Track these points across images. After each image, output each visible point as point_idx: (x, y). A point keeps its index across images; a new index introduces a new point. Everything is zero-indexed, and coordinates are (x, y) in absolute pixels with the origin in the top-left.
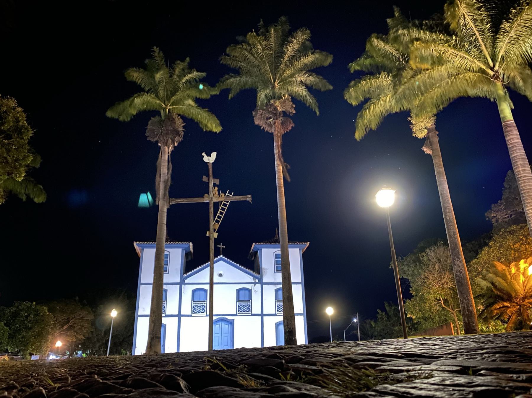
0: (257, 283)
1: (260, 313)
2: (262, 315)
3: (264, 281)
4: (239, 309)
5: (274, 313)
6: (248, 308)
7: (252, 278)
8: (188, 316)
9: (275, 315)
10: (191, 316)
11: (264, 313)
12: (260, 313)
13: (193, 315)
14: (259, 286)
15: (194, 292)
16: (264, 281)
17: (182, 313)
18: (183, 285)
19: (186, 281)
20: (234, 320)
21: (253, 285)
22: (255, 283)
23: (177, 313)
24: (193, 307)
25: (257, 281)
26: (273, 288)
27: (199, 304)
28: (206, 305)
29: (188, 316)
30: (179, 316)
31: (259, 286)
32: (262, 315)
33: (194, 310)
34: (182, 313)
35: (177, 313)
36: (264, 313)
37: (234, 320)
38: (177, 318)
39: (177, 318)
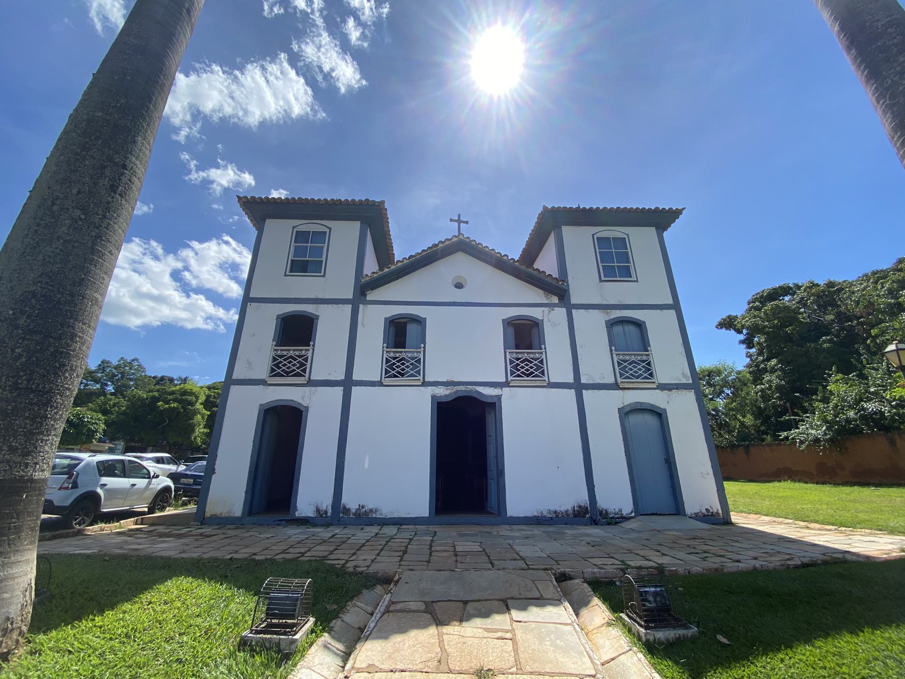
0: (555, 305)
1: (570, 379)
2: (578, 386)
3: (574, 301)
5: (611, 380)
6: (538, 368)
7: (541, 292)
8: (372, 384)
9: (615, 386)
10: (380, 384)
11: (584, 380)
12: (572, 381)
13: (387, 381)
14: (564, 310)
16: (574, 301)
17: (355, 377)
18: (361, 306)
19: (370, 297)
20: (499, 397)
21: (546, 309)
22: (551, 306)
24: (387, 361)
25: (555, 300)
28: (421, 356)
29: (372, 384)
30: (348, 383)
31: (561, 312)
34: (355, 377)
36: (584, 380)
37: (499, 397)
38: (339, 391)
39: (339, 391)
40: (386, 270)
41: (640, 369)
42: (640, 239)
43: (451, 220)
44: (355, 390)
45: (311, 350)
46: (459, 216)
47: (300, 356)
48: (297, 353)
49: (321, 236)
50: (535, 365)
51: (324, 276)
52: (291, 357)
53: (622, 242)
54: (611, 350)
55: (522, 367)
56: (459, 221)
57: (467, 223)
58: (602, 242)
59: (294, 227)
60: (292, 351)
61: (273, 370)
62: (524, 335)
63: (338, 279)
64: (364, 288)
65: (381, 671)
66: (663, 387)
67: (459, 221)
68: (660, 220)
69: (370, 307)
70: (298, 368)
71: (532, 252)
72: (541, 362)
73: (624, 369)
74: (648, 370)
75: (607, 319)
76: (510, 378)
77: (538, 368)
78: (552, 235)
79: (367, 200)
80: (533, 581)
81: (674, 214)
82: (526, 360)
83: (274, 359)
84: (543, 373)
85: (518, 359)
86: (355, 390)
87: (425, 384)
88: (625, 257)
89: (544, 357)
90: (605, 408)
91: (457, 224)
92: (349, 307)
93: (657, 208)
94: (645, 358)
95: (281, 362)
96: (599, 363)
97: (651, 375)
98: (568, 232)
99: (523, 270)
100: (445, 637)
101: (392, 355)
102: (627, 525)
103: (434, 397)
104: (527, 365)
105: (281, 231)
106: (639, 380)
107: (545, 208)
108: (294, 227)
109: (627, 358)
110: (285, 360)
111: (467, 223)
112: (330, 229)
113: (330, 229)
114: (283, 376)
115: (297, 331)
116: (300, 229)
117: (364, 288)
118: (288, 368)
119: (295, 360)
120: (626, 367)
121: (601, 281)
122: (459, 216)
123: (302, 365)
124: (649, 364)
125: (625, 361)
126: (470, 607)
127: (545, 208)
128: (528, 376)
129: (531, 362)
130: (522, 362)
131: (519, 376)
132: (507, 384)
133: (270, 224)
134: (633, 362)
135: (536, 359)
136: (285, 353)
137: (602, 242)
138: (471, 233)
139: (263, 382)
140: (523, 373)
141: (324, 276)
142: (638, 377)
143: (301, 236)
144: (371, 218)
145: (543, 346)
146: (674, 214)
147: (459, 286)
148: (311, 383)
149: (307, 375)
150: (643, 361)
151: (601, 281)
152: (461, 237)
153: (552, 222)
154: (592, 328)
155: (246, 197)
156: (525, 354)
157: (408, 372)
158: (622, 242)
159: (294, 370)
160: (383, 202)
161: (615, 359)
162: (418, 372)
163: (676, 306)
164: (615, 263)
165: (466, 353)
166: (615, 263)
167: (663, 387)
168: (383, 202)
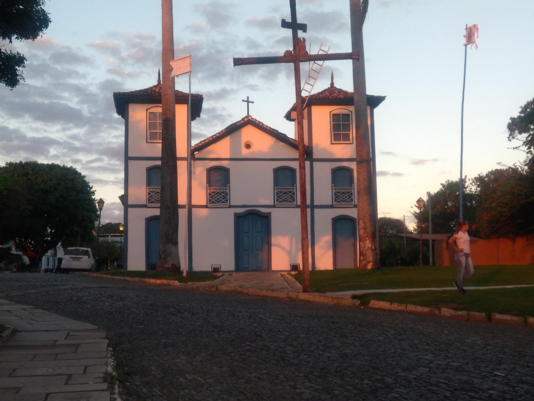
5: (329, 203)
9: (332, 207)
10: (206, 207)
11: (316, 203)
13: (209, 205)
15: (210, 171)
20: (270, 213)
26: (329, 167)
28: (228, 191)
37: (270, 213)
41: (346, 197)
43: (243, 101)
44: (194, 210)
46: (248, 98)
55: (283, 197)
56: (248, 102)
57: (253, 102)
58: (335, 117)
61: (149, 200)
67: (248, 102)
69: (198, 163)
72: (294, 194)
73: (337, 197)
75: (332, 168)
76: (276, 203)
77: (292, 197)
83: (149, 194)
84: (294, 200)
85: (281, 192)
87: (230, 207)
91: (246, 103)
94: (349, 190)
101: (212, 190)
103: (235, 214)
105: (139, 114)
106: (344, 203)
108: (147, 110)
111: (253, 102)
114: (155, 203)
121: (332, 144)
122: (248, 98)
125: (339, 192)
128: (285, 201)
131: (281, 202)
132: (274, 206)
134: (343, 193)
136: (154, 190)
138: (256, 115)
139: (145, 206)
142: (344, 201)
147: (248, 146)
150: (348, 192)
151: (332, 144)
152: (250, 118)
161: (334, 191)
162: (227, 200)
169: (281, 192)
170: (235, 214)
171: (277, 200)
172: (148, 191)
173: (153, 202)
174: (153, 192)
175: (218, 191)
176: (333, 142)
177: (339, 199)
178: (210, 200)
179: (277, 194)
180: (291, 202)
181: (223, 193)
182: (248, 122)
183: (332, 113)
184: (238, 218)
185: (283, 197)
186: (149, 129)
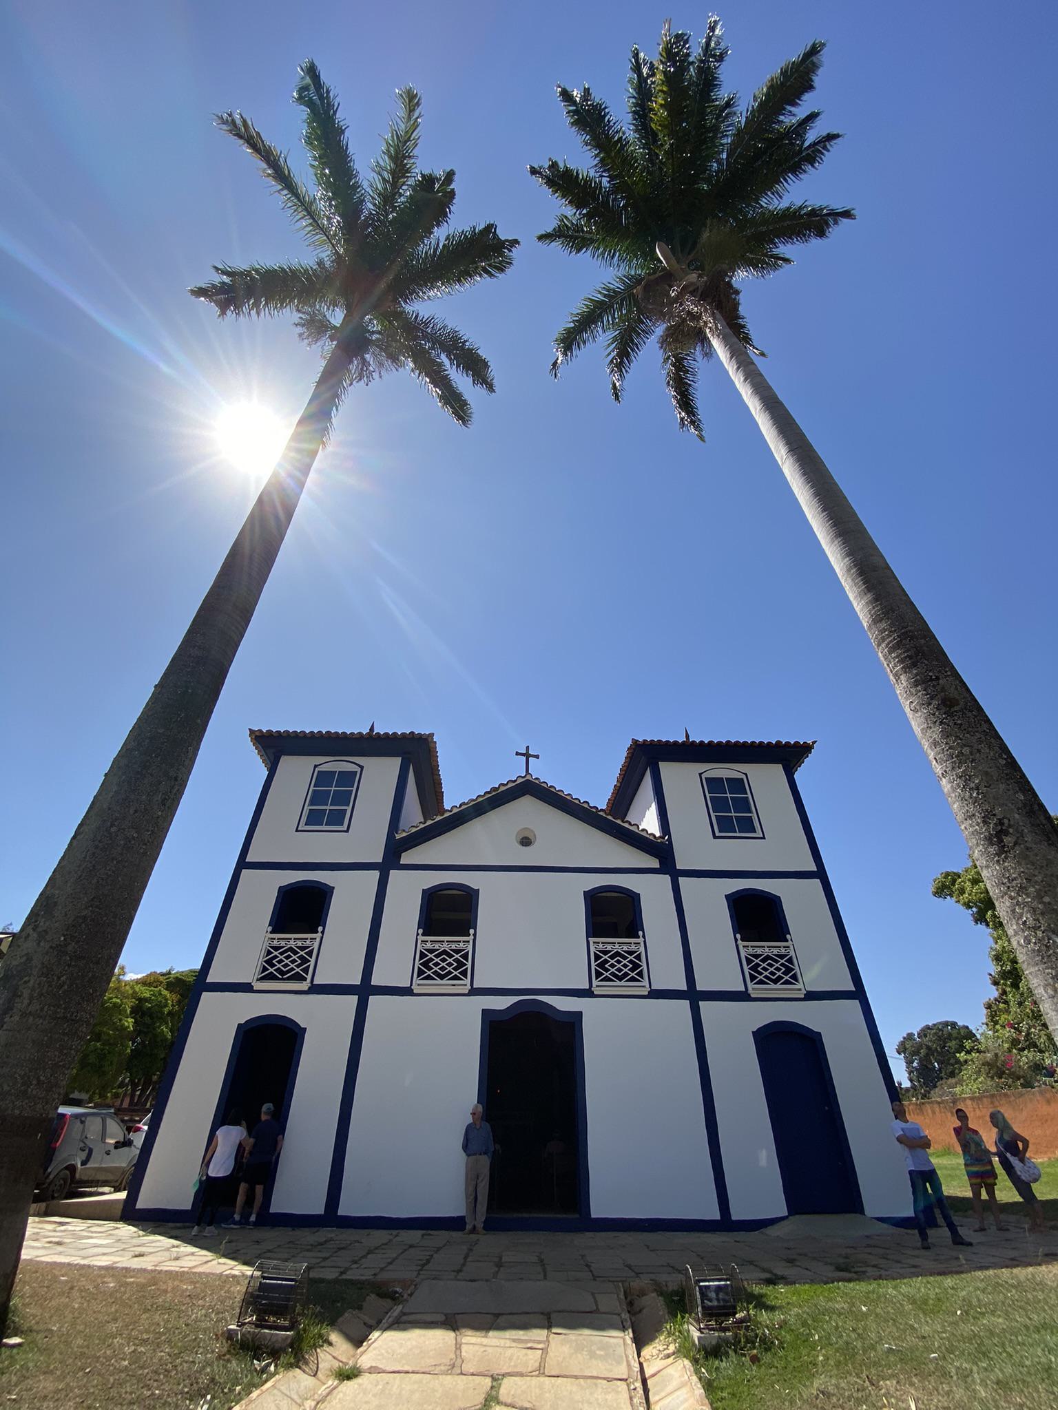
2: (693, 995)
4: (601, 966)
9: (743, 996)
10: (407, 992)
14: (668, 878)
17: (376, 980)
18: (393, 873)
19: (406, 859)
23: (357, 981)
24: (422, 955)
25: (655, 864)
27: (445, 942)
30: (365, 990)
32: (693, 995)
33: (426, 966)
34: (376, 980)
35: (357, 981)
40: (429, 822)
42: (765, 782)
43: (518, 754)
44: (373, 1000)
45: (318, 940)
47: (302, 948)
48: (300, 944)
49: (348, 779)
50: (631, 961)
51: (347, 831)
52: (291, 949)
53: (738, 785)
54: (736, 940)
55: (613, 966)
56: (527, 755)
57: (537, 757)
58: (714, 784)
59: (316, 766)
60: (292, 940)
61: (265, 969)
62: (612, 914)
63: (366, 834)
64: (395, 851)
65: (384, 1372)
66: (811, 996)
67: (527, 755)
68: (789, 756)
70: (298, 966)
71: (624, 796)
72: (639, 957)
73: (755, 968)
74: (788, 971)
76: (595, 983)
77: (636, 966)
78: (648, 773)
79: (412, 733)
80: (593, 1294)
81: (803, 750)
82: (617, 954)
83: (269, 953)
86: (373, 1000)
87: (474, 992)
88: (744, 805)
89: (642, 949)
90: (734, 1030)
92: (375, 875)
93: (778, 743)
94: (783, 951)
95: (276, 957)
96: (721, 959)
97: (795, 977)
98: (668, 770)
99: (612, 821)
100: (464, 1348)
101: (429, 946)
102: (772, 1231)
103: (486, 1013)
104: (619, 962)
105: (298, 772)
106: (778, 986)
107: (635, 742)
108: (316, 766)
109: (759, 951)
110: (281, 954)
112: (362, 767)
113: (362, 767)
115: (302, 908)
116: (323, 768)
117: (395, 851)
118: (287, 965)
119: (295, 953)
120: (758, 965)
121: (715, 837)
123: (304, 960)
124: (790, 961)
125: (757, 956)
126: (501, 1319)
127: (635, 742)
128: (620, 979)
129: (625, 958)
130: (612, 957)
132: (587, 993)
133: (288, 764)
134: (768, 958)
135: (631, 953)
136: (283, 943)
137: (714, 784)
138: (541, 772)
139: (246, 988)
140: (613, 974)
141: (347, 831)
143: (323, 778)
144: (415, 753)
145: (640, 933)
146: (803, 750)
147: (526, 842)
148: (316, 989)
149: (309, 977)
150: (782, 957)
152: (528, 777)
153: (646, 758)
154: (709, 905)
155: (260, 731)
156: (617, 944)
157: (450, 973)
158: (738, 785)
159: (292, 969)
160: (432, 735)
162: (464, 973)
163: (820, 874)
164: (732, 813)
165: (530, 943)
166: (732, 813)
167: (811, 996)
168: (432, 735)
169: (605, 953)
170: (486, 1013)
171: (598, 974)
172: (266, 944)
173: (271, 977)
174: (276, 949)
175: (445, 947)
176: (717, 834)
177: (761, 974)
178: (420, 972)
179: (597, 957)
180: (633, 979)
181: (457, 951)
182: (528, 788)
183: (703, 776)
184: (493, 1025)
185: (613, 966)
186: (311, 804)
